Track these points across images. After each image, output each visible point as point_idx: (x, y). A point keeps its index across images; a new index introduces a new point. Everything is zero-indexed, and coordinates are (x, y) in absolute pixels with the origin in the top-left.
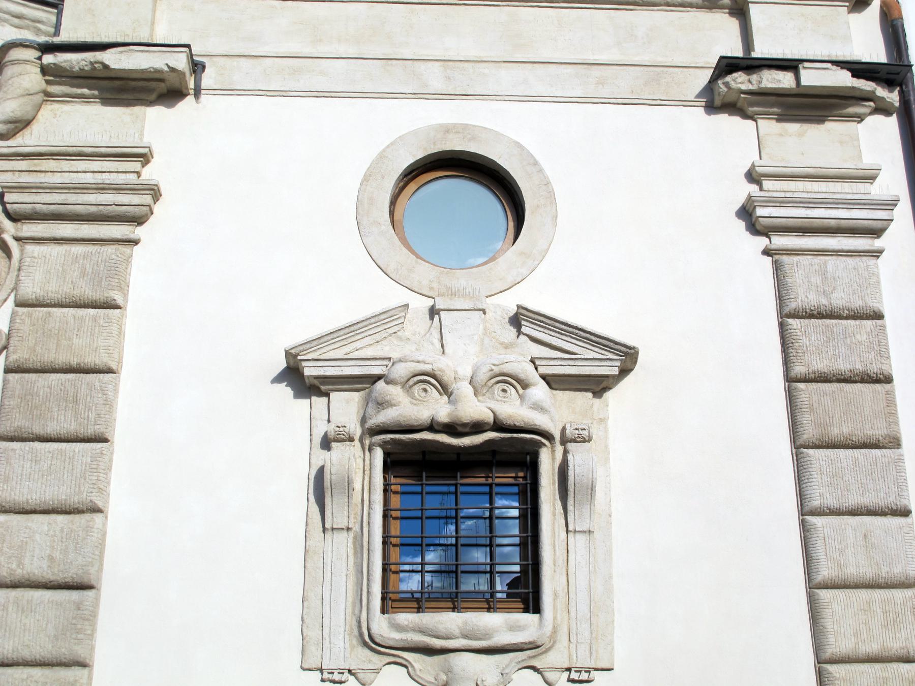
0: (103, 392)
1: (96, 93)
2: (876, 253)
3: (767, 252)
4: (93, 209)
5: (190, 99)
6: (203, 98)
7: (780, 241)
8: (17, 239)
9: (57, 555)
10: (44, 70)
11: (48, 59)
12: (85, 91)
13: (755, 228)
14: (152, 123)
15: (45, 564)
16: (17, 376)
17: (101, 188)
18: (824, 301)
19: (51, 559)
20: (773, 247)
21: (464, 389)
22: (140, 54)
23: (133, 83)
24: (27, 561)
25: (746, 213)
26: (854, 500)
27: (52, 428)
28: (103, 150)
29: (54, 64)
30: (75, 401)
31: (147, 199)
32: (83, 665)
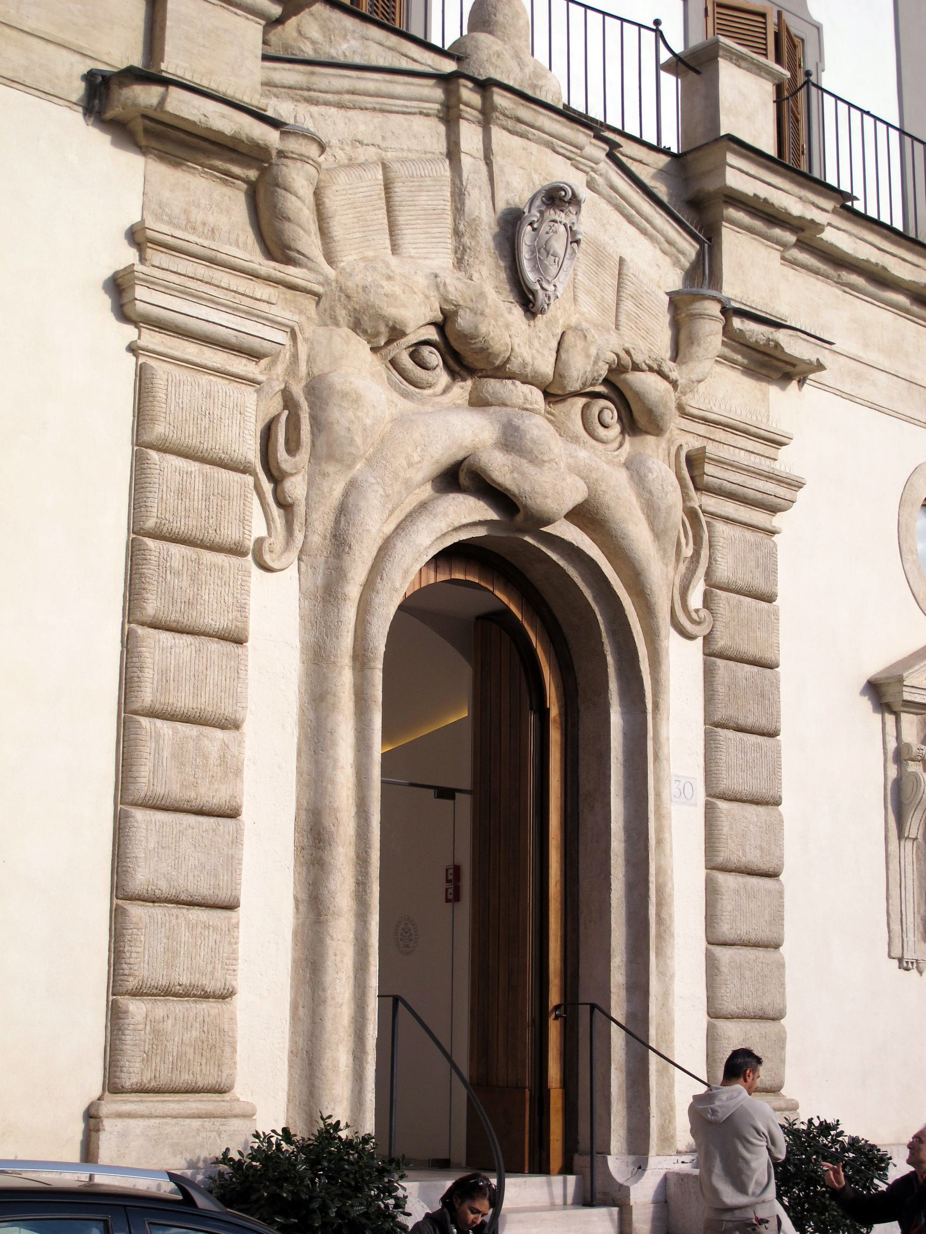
1: (745, 361)
3: (133, 349)
4: (759, 496)
5: (794, 383)
7: (151, 339)
8: (704, 512)
9: (764, 845)
10: (727, 330)
11: (737, 323)
12: (739, 358)
13: (124, 312)
14: (780, 406)
15: (758, 853)
19: (762, 849)
20: (141, 343)
22: (801, 341)
23: (775, 362)
25: (119, 288)
28: (762, 433)
29: (741, 330)
30: (763, 696)
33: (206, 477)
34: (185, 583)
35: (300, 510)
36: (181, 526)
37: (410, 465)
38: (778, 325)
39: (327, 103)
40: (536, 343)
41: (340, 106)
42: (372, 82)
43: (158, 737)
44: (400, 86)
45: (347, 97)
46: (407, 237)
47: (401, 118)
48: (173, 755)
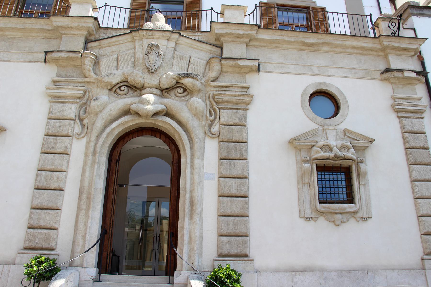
0: (245, 148)
2: (422, 118)
6: (260, 73)
9: (239, 188)
16: (223, 143)
17: (239, 95)
18: (413, 129)
19: (237, 189)
21: (335, 149)
24: (231, 190)
26: (424, 177)
27: (233, 157)
30: (239, 150)
31: (251, 99)
32: (247, 217)
33: (60, 122)
34: (52, 143)
35: (86, 125)
36: (53, 133)
37: (111, 111)
38: (238, 59)
39: (106, 47)
40: (153, 79)
41: (109, 46)
42: (114, 39)
43: (41, 174)
44: (120, 38)
45: (110, 44)
46: (120, 66)
47: (124, 44)
48: (44, 178)
